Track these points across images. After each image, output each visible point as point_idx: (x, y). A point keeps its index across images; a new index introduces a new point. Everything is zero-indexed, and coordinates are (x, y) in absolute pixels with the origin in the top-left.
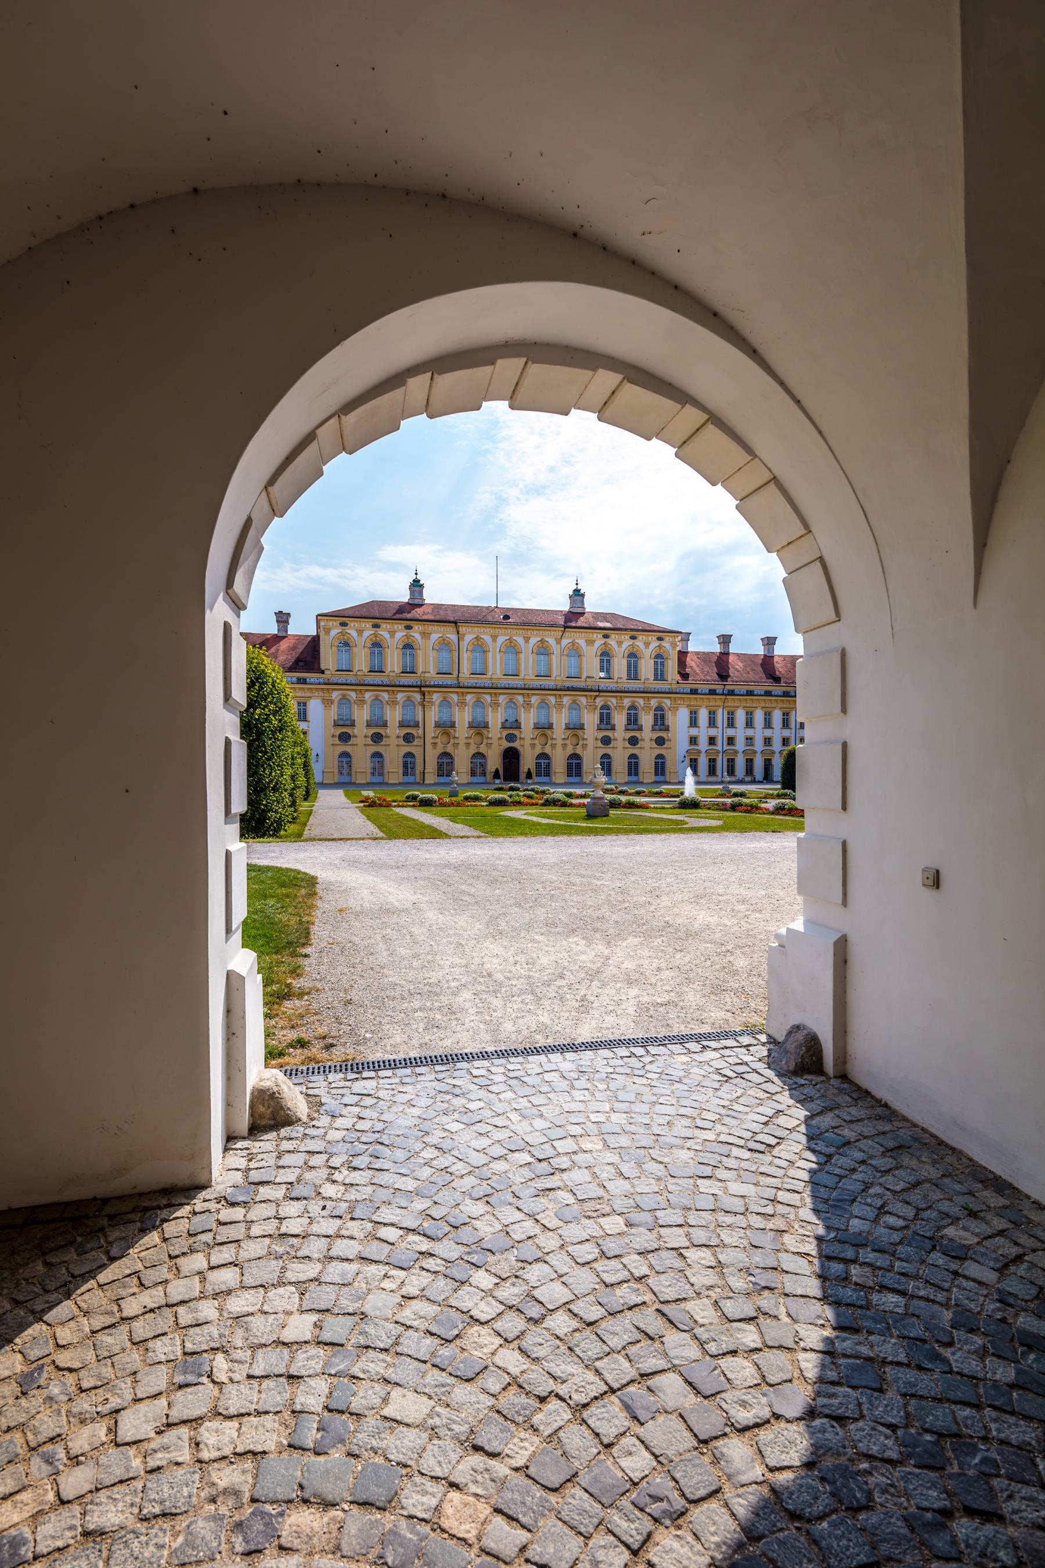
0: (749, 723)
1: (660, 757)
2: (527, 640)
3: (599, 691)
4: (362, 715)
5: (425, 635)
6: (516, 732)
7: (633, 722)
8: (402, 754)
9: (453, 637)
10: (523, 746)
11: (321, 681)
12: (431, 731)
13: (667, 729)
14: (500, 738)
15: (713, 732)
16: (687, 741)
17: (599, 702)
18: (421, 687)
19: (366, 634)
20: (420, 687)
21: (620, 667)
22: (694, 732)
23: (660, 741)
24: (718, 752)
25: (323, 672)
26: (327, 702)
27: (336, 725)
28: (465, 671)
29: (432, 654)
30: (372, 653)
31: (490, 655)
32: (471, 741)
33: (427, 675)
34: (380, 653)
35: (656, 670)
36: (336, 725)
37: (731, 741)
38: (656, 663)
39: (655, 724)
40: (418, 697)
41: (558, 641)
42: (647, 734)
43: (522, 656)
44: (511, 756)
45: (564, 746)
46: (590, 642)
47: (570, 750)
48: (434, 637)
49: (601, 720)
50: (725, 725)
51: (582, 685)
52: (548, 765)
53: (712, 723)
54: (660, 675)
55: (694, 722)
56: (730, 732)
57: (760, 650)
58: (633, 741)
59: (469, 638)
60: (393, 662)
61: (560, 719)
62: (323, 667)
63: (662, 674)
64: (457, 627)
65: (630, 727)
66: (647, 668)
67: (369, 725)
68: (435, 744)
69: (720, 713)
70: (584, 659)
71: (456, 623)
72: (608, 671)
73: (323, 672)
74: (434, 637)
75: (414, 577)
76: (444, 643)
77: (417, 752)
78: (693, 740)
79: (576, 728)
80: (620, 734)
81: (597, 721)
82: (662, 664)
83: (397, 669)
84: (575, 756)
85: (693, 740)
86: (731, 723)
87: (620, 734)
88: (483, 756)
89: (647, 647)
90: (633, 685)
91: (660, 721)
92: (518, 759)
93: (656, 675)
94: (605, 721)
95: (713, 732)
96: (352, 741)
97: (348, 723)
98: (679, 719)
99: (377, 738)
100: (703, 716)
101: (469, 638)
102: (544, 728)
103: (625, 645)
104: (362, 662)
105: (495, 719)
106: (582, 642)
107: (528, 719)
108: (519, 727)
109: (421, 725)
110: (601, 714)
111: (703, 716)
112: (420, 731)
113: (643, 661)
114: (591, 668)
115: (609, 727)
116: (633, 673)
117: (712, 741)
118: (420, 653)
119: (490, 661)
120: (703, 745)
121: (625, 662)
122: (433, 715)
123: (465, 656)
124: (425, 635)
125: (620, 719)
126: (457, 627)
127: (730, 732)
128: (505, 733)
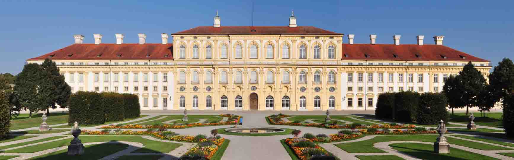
0: (381, 80)
7: (318, 78)
13: (335, 83)
15: (361, 84)
20: (213, 65)
21: (310, 53)
22: (350, 84)
24: (363, 95)
26: (175, 73)
35: (329, 54)
36: (179, 84)
37: (371, 89)
40: (212, 70)
44: (254, 98)
50: (367, 80)
51: (291, 63)
53: (360, 79)
54: (332, 55)
55: (350, 80)
56: (370, 84)
66: (325, 53)
69: (364, 74)
78: (350, 89)
80: (310, 85)
81: (298, 79)
83: (204, 58)
85: (350, 89)
86: (371, 80)
87: (310, 85)
91: (332, 78)
92: (257, 100)
95: (361, 84)
98: (342, 77)
99: (196, 89)
100: (355, 77)
111: (355, 77)
112: (214, 86)
114: (295, 53)
116: (317, 55)
117: (361, 89)
120: (355, 91)
127: (370, 84)
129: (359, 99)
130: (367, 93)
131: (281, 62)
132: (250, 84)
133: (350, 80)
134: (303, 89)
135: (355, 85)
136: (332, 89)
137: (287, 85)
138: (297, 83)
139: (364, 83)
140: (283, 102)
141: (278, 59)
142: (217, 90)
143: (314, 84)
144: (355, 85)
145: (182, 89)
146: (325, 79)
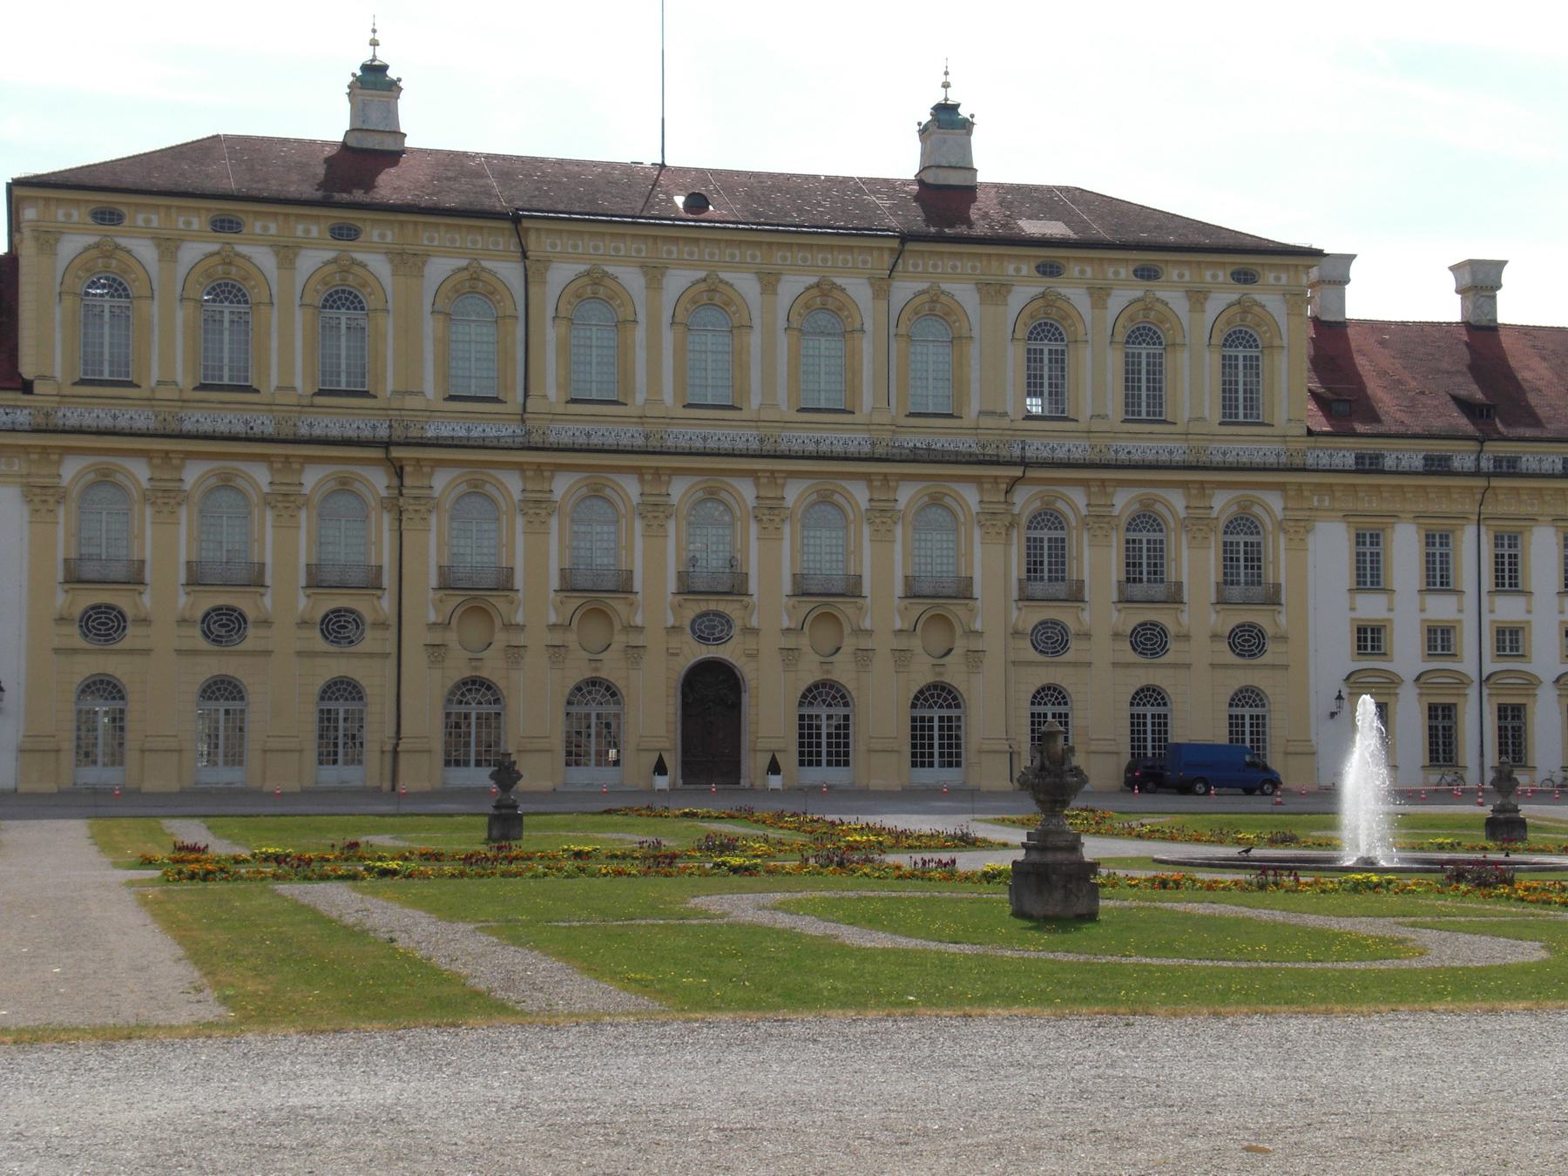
1: (1247, 696)
2: (769, 281)
3: (1024, 463)
4: (166, 545)
5: (408, 261)
6: (729, 607)
7: (1144, 569)
8: (320, 683)
9: (509, 272)
10: (753, 656)
11: (22, 417)
12: (424, 606)
13: (1273, 599)
14: (673, 630)
15: (1441, 608)
16: (1347, 640)
17: (1025, 500)
18: (394, 450)
19: (192, 253)
20: (387, 444)
22: (1371, 607)
23: (1247, 641)
24: (1462, 681)
25: (27, 387)
27: (74, 578)
28: (552, 393)
29: (430, 326)
30: (213, 321)
31: (640, 334)
32: (451, 638)
33: (410, 402)
34: (241, 322)
35: (1228, 388)
37: (1510, 639)
38: (1228, 363)
39: (1228, 580)
40: (378, 481)
41: (881, 287)
42: (1200, 618)
43: (755, 340)
44: (711, 697)
45: (902, 657)
46: (995, 291)
47: (922, 674)
48: (440, 268)
49: (1033, 568)
51: (965, 444)
52: (842, 731)
53: (1438, 577)
54: (1240, 403)
55: (1369, 573)
56: (1508, 609)
57: (1447, 308)
58: (1149, 640)
59: (561, 274)
60: (287, 358)
61: (883, 563)
62: (27, 369)
63: (1251, 402)
64: (520, 234)
65: (1137, 590)
66: (1194, 385)
67: (196, 579)
68: (436, 651)
70: (974, 350)
71: (516, 219)
72: (1056, 396)
73: (27, 387)
74: (440, 268)
75: (365, 56)
76: (473, 285)
77: (374, 679)
79: (939, 601)
80: (1102, 616)
81: (1017, 569)
82: (1252, 365)
84: (939, 693)
86: (1508, 575)
87: (1102, 616)
88: (612, 692)
89: (1194, 309)
90: (1145, 444)
92: (736, 707)
93: (1228, 404)
94: (1046, 566)
95: (1441, 608)
96: (133, 637)
97: (118, 572)
99: (224, 625)
100: (1405, 550)
101: (561, 274)
102: (826, 599)
103: (1119, 300)
104: (168, 354)
105: (654, 560)
106: (965, 294)
107: (772, 563)
108: (738, 589)
109: (388, 579)
110: (1033, 545)
111: (1405, 550)
112: (386, 604)
113: (1183, 357)
115: (1060, 589)
116: (1144, 393)
117: (1439, 639)
118: (389, 325)
119: (641, 356)
121: (1114, 361)
122: (430, 547)
123: (550, 335)
124: (408, 261)
125: (1098, 563)
126: (520, 234)
127: (1508, 609)
128: (693, 609)
129: (1432, 708)
130: (1489, 668)
131: (913, 440)
132: (687, 589)
133: (1369, 573)
134: (1052, 640)
135: (1406, 610)
136: (1247, 641)
137: (939, 601)
138: (1015, 594)
139: (1470, 601)
140: (919, 729)
141: (885, 419)
142: (415, 637)
143: (1125, 600)
144: (1406, 610)
145: (103, 624)
146: (1195, 565)
